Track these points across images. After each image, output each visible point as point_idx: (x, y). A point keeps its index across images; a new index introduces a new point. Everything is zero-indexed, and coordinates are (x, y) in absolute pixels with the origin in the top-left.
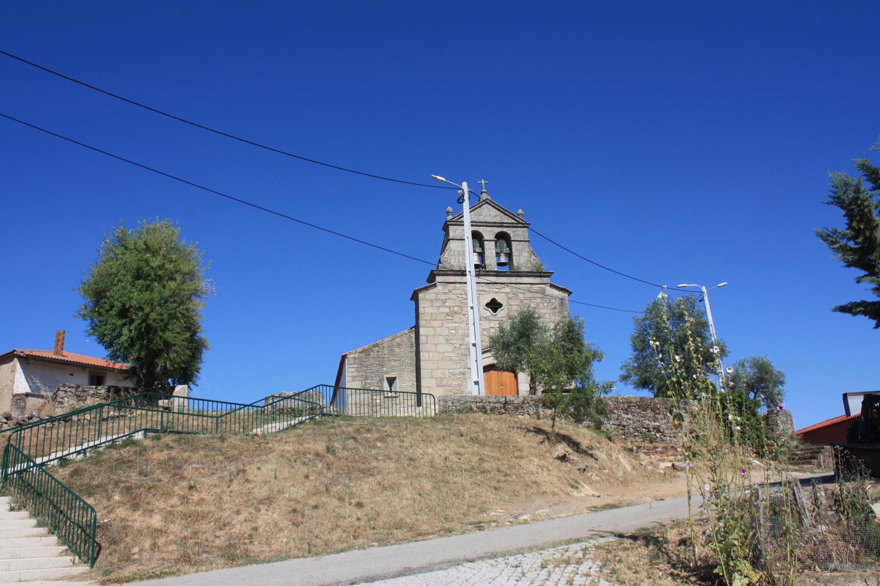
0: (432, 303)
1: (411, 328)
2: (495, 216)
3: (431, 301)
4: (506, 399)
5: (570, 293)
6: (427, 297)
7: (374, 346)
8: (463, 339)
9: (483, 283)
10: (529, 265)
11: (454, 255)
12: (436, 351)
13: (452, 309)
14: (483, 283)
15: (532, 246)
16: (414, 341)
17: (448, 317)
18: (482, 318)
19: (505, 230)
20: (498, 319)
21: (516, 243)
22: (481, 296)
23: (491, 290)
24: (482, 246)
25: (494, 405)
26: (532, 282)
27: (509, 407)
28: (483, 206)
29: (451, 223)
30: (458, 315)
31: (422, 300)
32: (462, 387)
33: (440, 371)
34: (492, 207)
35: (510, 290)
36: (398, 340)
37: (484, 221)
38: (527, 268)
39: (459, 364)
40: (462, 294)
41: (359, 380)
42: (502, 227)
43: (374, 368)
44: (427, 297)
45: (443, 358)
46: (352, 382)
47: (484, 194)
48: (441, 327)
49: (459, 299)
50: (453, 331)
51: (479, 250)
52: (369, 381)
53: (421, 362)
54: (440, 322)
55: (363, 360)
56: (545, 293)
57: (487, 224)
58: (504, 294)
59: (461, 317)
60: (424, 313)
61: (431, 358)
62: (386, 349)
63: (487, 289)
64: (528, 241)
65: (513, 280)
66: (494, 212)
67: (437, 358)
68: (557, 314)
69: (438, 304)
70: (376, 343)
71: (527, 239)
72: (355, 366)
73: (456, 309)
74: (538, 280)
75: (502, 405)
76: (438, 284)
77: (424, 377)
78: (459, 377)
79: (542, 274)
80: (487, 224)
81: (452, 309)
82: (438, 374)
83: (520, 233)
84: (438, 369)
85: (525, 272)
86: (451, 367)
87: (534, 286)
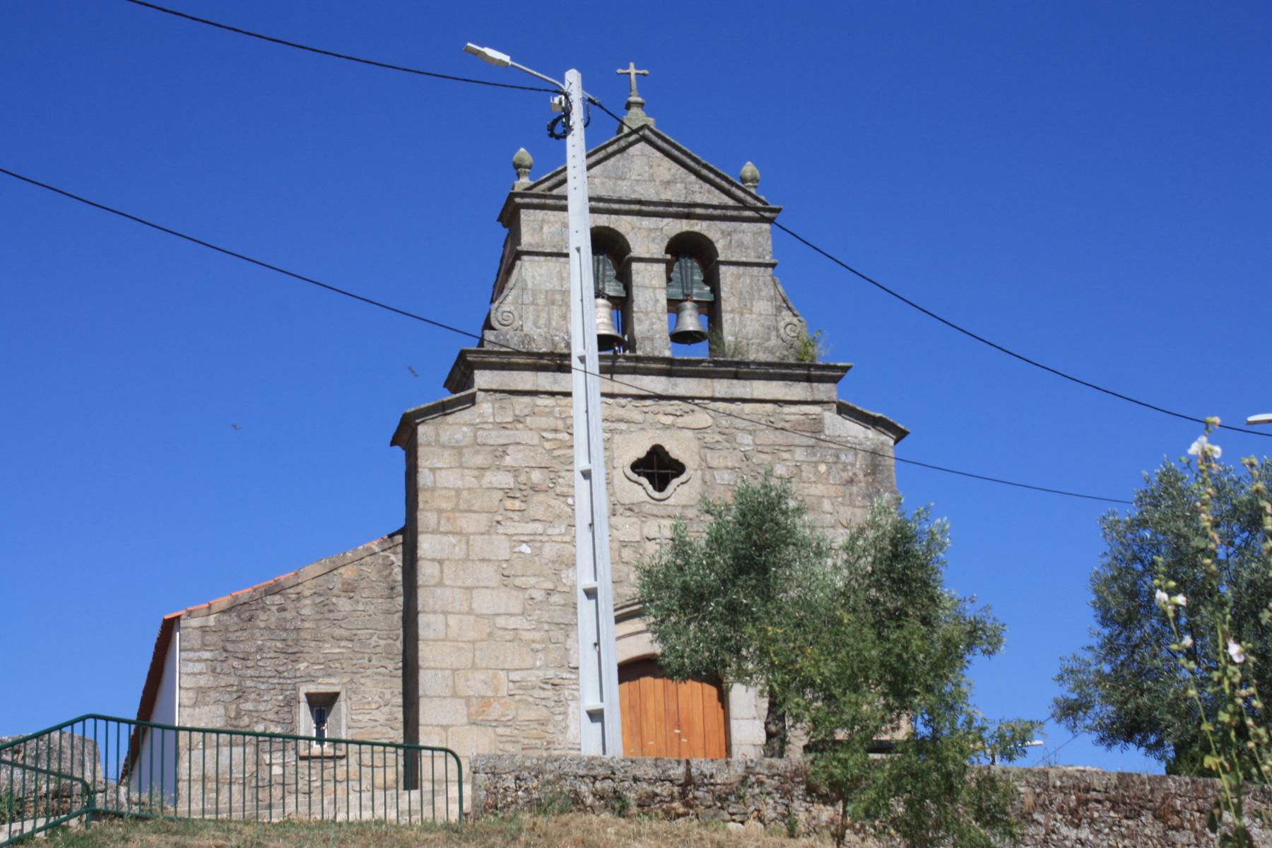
0: (460, 454)
1: (391, 536)
2: (669, 182)
3: (458, 449)
4: (688, 770)
5: (900, 434)
6: (444, 437)
7: (270, 591)
8: (557, 573)
9: (625, 396)
10: (773, 342)
12: (470, 612)
13: (523, 478)
14: (625, 396)
15: (784, 286)
16: (400, 578)
17: (509, 504)
18: (620, 509)
19: (699, 227)
20: (669, 511)
21: (733, 269)
23: (650, 417)
24: (624, 277)
25: (649, 789)
27: (699, 794)
28: (632, 150)
29: (527, 200)
30: (541, 497)
31: (429, 445)
32: (550, 728)
33: (481, 676)
34: (658, 154)
35: (710, 421)
36: (348, 573)
37: (634, 196)
38: (766, 350)
39: (540, 655)
40: (556, 431)
41: (217, 702)
42: (688, 216)
43: (269, 662)
44: (444, 437)
45: (490, 634)
46: (194, 706)
47: (635, 111)
48: (488, 533)
49: (548, 445)
50: (525, 549)
51: (613, 289)
52: (249, 706)
53: (421, 646)
54: (484, 518)
55: (233, 637)
56: (821, 431)
57: (642, 208)
58: (689, 434)
59: (553, 502)
60: (433, 489)
61: (454, 632)
62: (307, 602)
63: (637, 416)
64: (773, 266)
65: (721, 387)
66: (667, 168)
67: (472, 635)
68: (859, 501)
69: (479, 460)
70: (277, 583)
71: (768, 259)
72: (207, 655)
73: (536, 476)
74: (798, 390)
75: (676, 789)
76: (480, 395)
77: (428, 693)
78: (543, 694)
79: (814, 372)
80: (642, 208)
81: (523, 478)
82: (475, 684)
83: (747, 239)
84: (474, 667)
85: (760, 364)
86: (517, 664)
87: (788, 409)
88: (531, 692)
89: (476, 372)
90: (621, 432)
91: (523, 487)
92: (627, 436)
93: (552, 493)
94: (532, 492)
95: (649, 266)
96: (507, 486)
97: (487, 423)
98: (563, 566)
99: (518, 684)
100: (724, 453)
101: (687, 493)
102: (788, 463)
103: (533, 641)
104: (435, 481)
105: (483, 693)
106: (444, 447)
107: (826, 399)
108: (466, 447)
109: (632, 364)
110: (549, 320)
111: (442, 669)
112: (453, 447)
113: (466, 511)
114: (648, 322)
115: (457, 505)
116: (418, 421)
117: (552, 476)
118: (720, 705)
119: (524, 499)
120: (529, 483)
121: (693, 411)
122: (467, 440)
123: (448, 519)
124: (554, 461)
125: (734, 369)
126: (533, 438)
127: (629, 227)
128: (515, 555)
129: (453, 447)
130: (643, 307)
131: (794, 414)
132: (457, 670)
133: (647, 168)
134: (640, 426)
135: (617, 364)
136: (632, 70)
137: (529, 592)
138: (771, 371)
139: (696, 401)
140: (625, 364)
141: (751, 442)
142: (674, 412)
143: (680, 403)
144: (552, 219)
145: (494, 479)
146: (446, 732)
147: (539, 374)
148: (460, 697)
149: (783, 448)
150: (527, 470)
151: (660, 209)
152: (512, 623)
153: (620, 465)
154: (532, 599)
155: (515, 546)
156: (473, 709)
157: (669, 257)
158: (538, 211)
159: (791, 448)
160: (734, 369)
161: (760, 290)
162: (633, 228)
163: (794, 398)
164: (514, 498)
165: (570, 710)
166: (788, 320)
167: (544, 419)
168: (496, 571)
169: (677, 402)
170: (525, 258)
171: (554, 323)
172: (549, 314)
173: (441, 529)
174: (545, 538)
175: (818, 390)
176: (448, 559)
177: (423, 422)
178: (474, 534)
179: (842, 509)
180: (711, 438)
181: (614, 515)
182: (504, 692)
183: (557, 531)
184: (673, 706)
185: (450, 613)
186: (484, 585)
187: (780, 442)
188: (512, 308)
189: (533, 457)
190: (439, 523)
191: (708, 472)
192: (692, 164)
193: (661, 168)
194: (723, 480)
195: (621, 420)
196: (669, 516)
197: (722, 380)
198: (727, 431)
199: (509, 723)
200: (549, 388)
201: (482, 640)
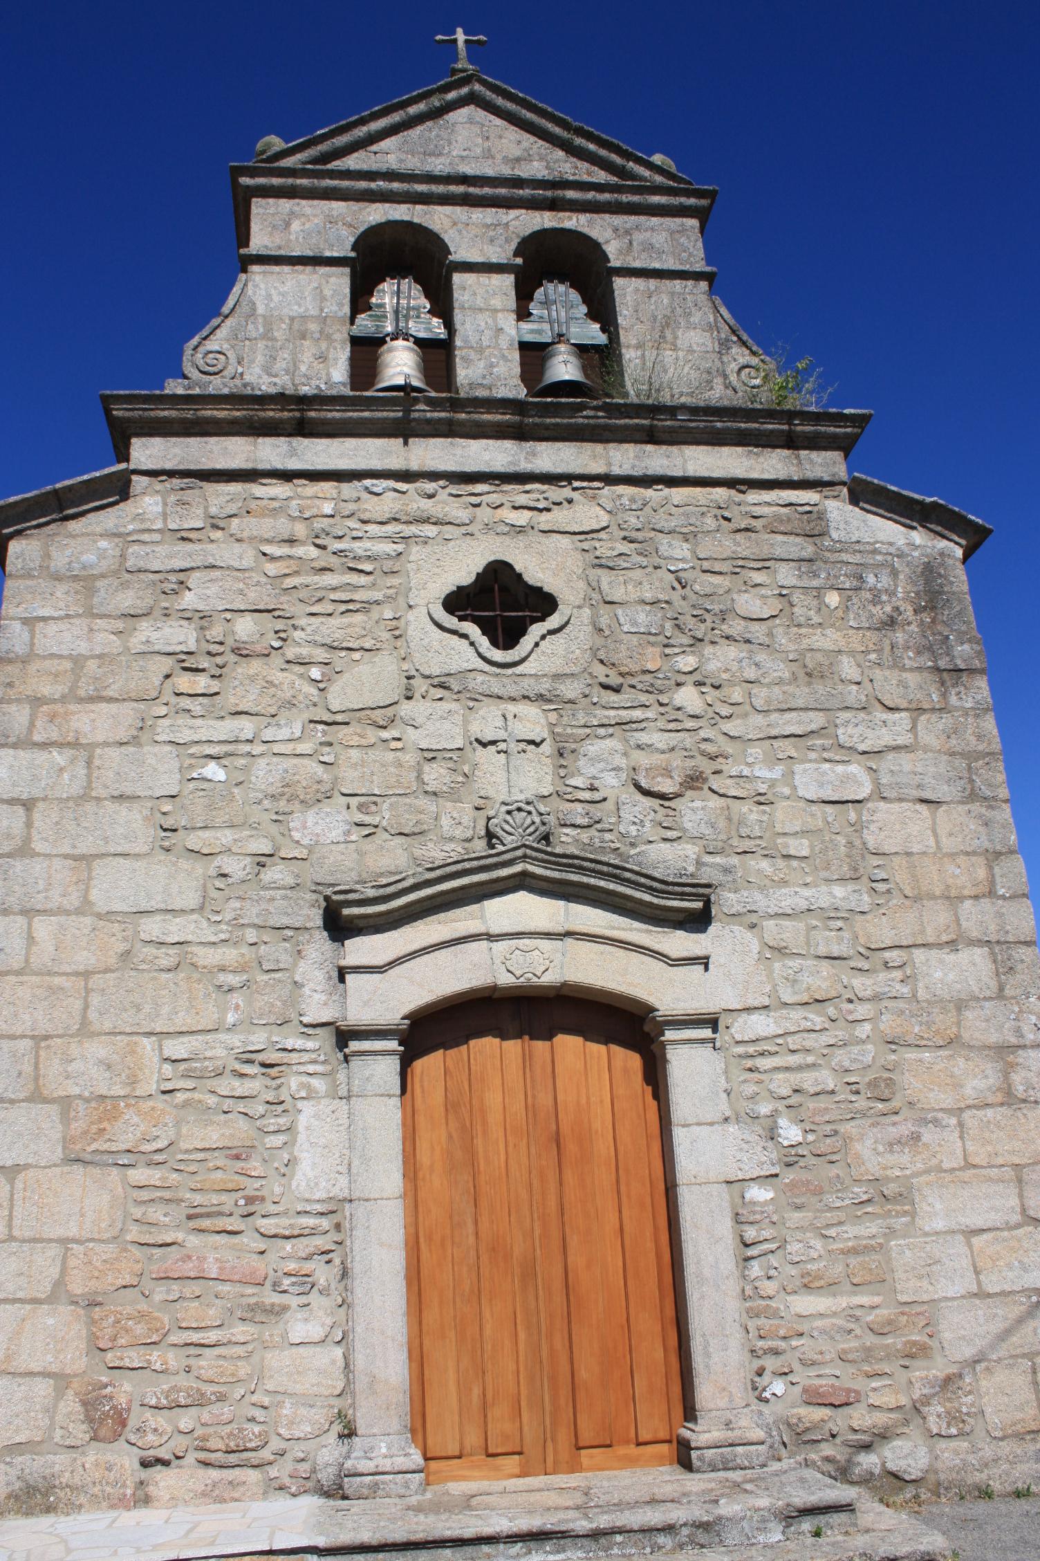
0: (91, 591)
3: (85, 581)
6: (60, 560)
9: (433, 476)
11: (267, 336)
13: (216, 632)
17: (184, 682)
18: (420, 685)
20: (528, 686)
22: (416, 552)
23: (484, 514)
26: (740, 473)
28: (453, 116)
30: (255, 666)
32: (255, 1166)
33: (98, 1049)
34: (498, 121)
39: (237, 998)
40: (291, 541)
42: (553, 205)
48: (135, 741)
49: (272, 569)
50: (213, 771)
54: (128, 713)
58: (565, 541)
59: (278, 677)
61: (45, 951)
67: (84, 959)
68: (909, 656)
69: (127, 600)
73: (245, 627)
74: (773, 464)
76: (139, 482)
78: (240, 1087)
81: (216, 632)
83: (659, 239)
84: (85, 1030)
85: (694, 411)
86: (183, 1020)
87: (753, 496)
88: (210, 1084)
89: (134, 440)
90: (426, 541)
91: (215, 648)
92: (437, 549)
93: (277, 660)
94: (237, 658)
95: (484, 279)
96: (178, 648)
97: (149, 531)
98: (297, 806)
99: (183, 1066)
100: (637, 575)
101: (561, 652)
102: (763, 591)
103: (223, 969)
104: (32, 644)
105: (104, 1093)
106: (57, 578)
107: (826, 478)
108: (103, 576)
109: (443, 415)
110: (295, 363)
111: (13, 1037)
112: (76, 578)
113: (91, 699)
114: (482, 364)
115: (73, 689)
116: (6, 531)
117: (280, 625)
118: (649, 1089)
119: (218, 672)
120: (230, 642)
121: (570, 501)
122: (104, 563)
123: (52, 718)
124: (284, 599)
126: (246, 556)
127: (447, 223)
128: (192, 785)
129: (76, 578)
130: (473, 340)
131: (769, 504)
132: (47, 1037)
133: (480, 141)
134: (463, 530)
135: (415, 415)
136: (460, 36)
137: (217, 861)
138: (719, 425)
139: (576, 484)
140: (429, 415)
141: (688, 554)
142: (532, 504)
143: (546, 487)
144: (308, 211)
145: (154, 636)
146: (12, 1182)
147: (260, 440)
148: (46, 1101)
149: (752, 565)
150: (228, 615)
151: (503, 191)
152: (176, 929)
153: (423, 602)
154: (224, 875)
155: (191, 766)
156: (77, 1127)
157: (519, 261)
158: (282, 201)
159: (767, 564)
162: (455, 224)
163: (766, 476)
164: (197, 670)
165: (302, 1121)
166: (742, 361)
167: (268, 522)
168: (146, 819)
170: (255, 268)
171: (303, 368)
172: (294, 354)
173: (37, 738)
174: (258, 749)
175: (811, 461)
176: (45, 799)
177: (18, 533)
178: (106, 744)
179: (878, 674)
180: (608, 547)
181: (409, 698)
182: (150, 1085)
183: (284, 733)
184: (545, 1100)
185: (39, 912)
186: (120, 850)
187: (745, 554)
188: (226, 346)
189: (241, 592)
190: (32, 724)
191: (604, 610)
192: (557, 130)
193: (503, 141)
194: (635, 624)
195: (426, 520)
196: (525, 697)
197: (626, 446)
198: (639, 536)
199: (159, 1158)
200: (279, 464)
201: (107, 970)
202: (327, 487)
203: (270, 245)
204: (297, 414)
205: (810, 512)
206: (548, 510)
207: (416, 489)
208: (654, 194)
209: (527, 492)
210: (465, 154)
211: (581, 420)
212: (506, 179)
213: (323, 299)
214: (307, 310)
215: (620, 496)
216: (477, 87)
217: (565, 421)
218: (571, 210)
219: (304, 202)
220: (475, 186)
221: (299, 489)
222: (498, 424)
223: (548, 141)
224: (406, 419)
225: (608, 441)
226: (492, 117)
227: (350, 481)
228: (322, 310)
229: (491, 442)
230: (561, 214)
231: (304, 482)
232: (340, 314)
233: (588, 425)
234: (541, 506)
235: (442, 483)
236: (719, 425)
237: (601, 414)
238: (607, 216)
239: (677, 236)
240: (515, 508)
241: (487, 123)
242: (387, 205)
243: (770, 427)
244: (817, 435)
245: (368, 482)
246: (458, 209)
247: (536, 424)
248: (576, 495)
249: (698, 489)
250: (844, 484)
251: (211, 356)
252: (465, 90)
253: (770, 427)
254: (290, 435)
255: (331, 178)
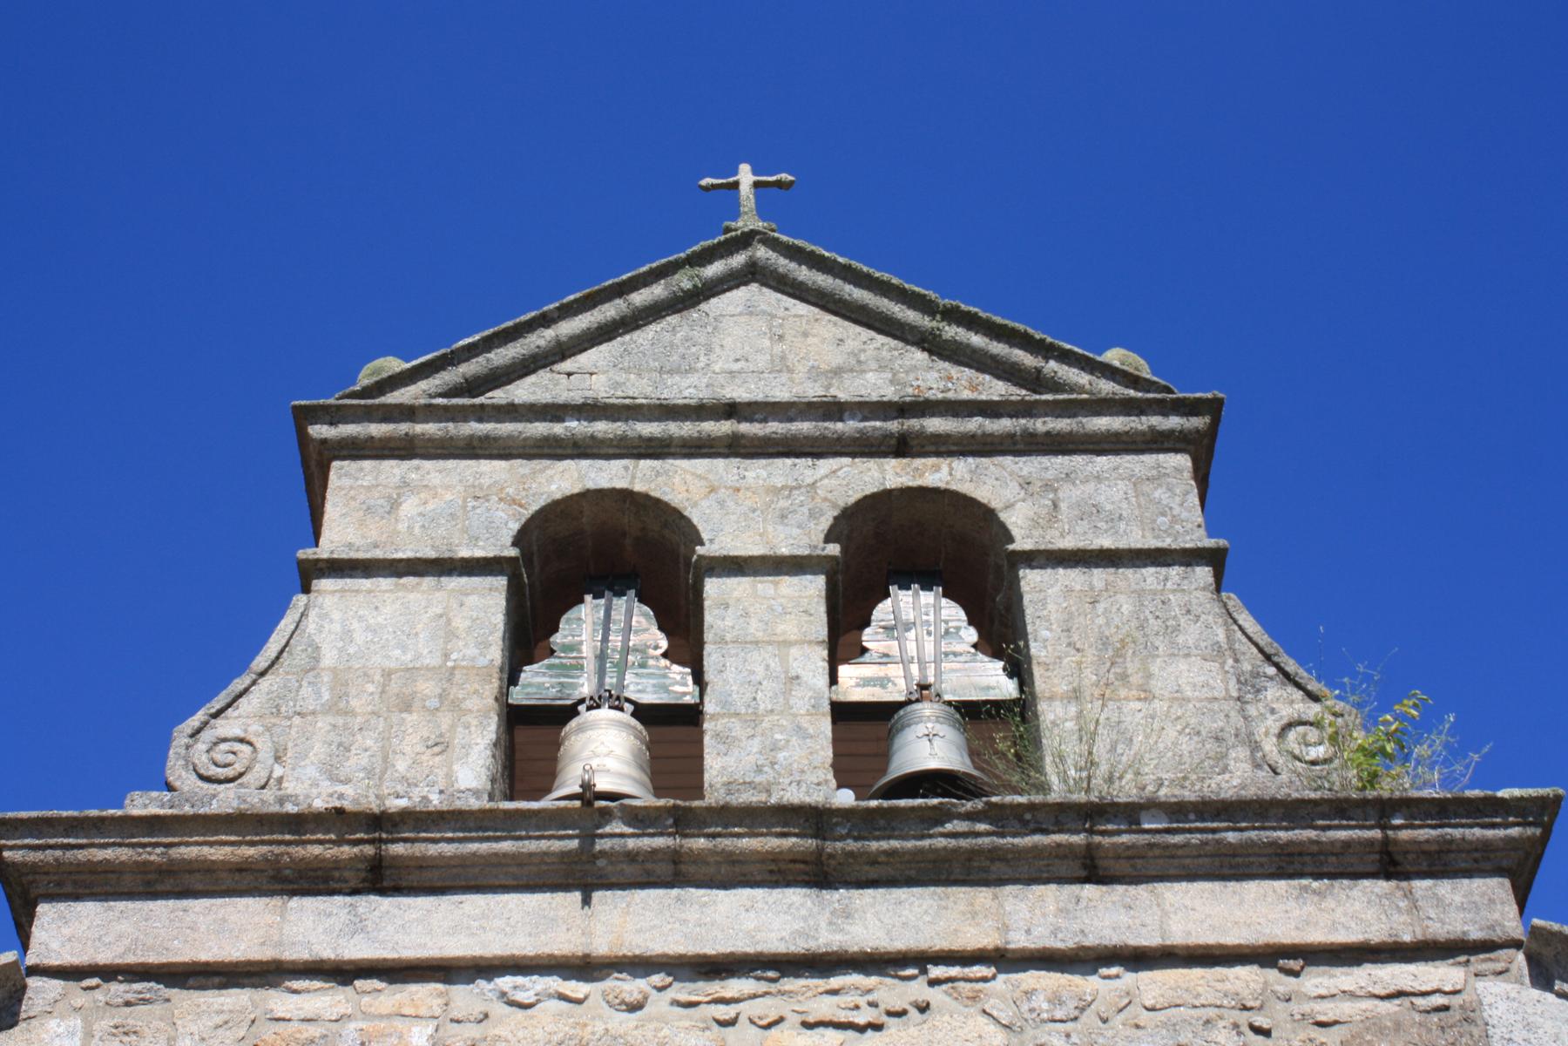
9: (640, 965)
28: (715, 305)
42: (902, 447)
64: (1214, 559)
76: (40, 991)
79: (1408, 834)
85: (1177, 810)
87: (1318, 980)
89: (43, 909)
95: (764, 586)
107: (1475, 934)
109: (660, 842)
114: (755, 746)
125: (1078, 839)
127: (698, 488)
130: (740, 703)
131: (1352, 995)
133: (767, 343)
135: (602, 845)
138: (1231, 837)
139: (936, 971)
140: (631, 843)
142: (843, 1016)
143: (873, 980)
147: (295, 902)
151: (804, 427)
157: (834, 549)
158: (388, 465)
160: (1078, 839)
161: (1172, 631)
166: (1287, 712)
169: (855, 979)
170: (324, 584)
171: (401, 766)
172: (385, 738)
175: (1439, 902)
188: (255, 727)
192: (911, 316)
193: (810, 340)
197: (1039, 889)
202: (424, 994)
203: (358, 542)
204: (369, 850)
205: (1446, 1008)
206: (877, 1027)
207: (604, 994)
208: (1099, 414)
209: (834, 992)
210: (736, 367)
211: (941, 842)
212: (810, 405)
213: (451, 635)
214: (418, 657)
215: (1029, 994)
216: (762, 252)
217: (910, 844)
218: (938, 454)
219: (428, 464)
220: (751, 420)
221: (366, 999)
222: (774, 857)
223: (895, 337)
224: (586, 855)
225: (1001, 882)
226: (790, 302)
227: (471, 981)
228: (446, 656)
229: (759, 893)
230: (919, 462)
231: (375, 984)
232: (482, 662)
233: (956, 851)
234: (861, 1018)
235: (658, 979)
236: (1231, 837)
237: (982, 827)
238: (1008, 461)
239: (1147, 487)
240: (808, 1025)
241: (781, 313)
242: (585, 463)
243: (1342, 835)
244: (1447, 846)
245: (505, 982)
246: (720, 463)
247: (851, 854)
248: (936, 995)
249: (1197, 972)
250: (1517, 944)
251: (224, 747)
252: (738, 260)
253: (1342, 835)
254: (354, 892)
255: (480, 420)
